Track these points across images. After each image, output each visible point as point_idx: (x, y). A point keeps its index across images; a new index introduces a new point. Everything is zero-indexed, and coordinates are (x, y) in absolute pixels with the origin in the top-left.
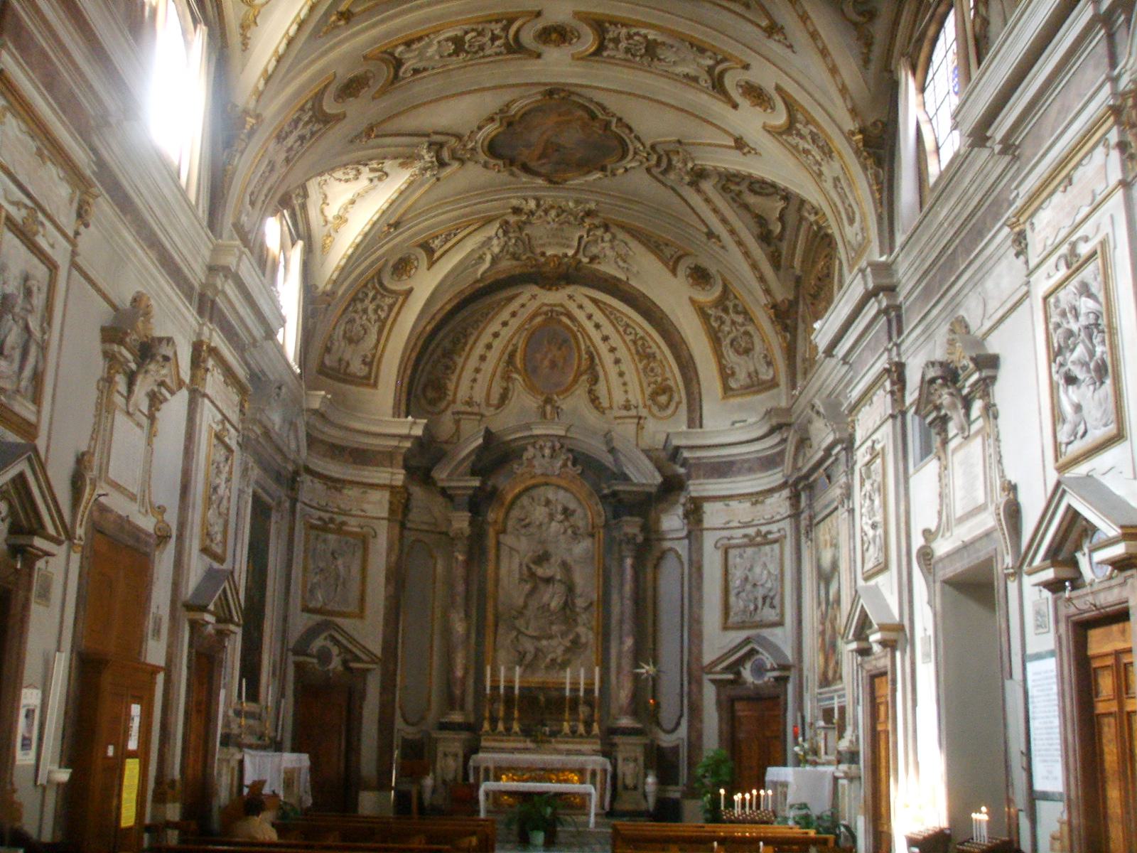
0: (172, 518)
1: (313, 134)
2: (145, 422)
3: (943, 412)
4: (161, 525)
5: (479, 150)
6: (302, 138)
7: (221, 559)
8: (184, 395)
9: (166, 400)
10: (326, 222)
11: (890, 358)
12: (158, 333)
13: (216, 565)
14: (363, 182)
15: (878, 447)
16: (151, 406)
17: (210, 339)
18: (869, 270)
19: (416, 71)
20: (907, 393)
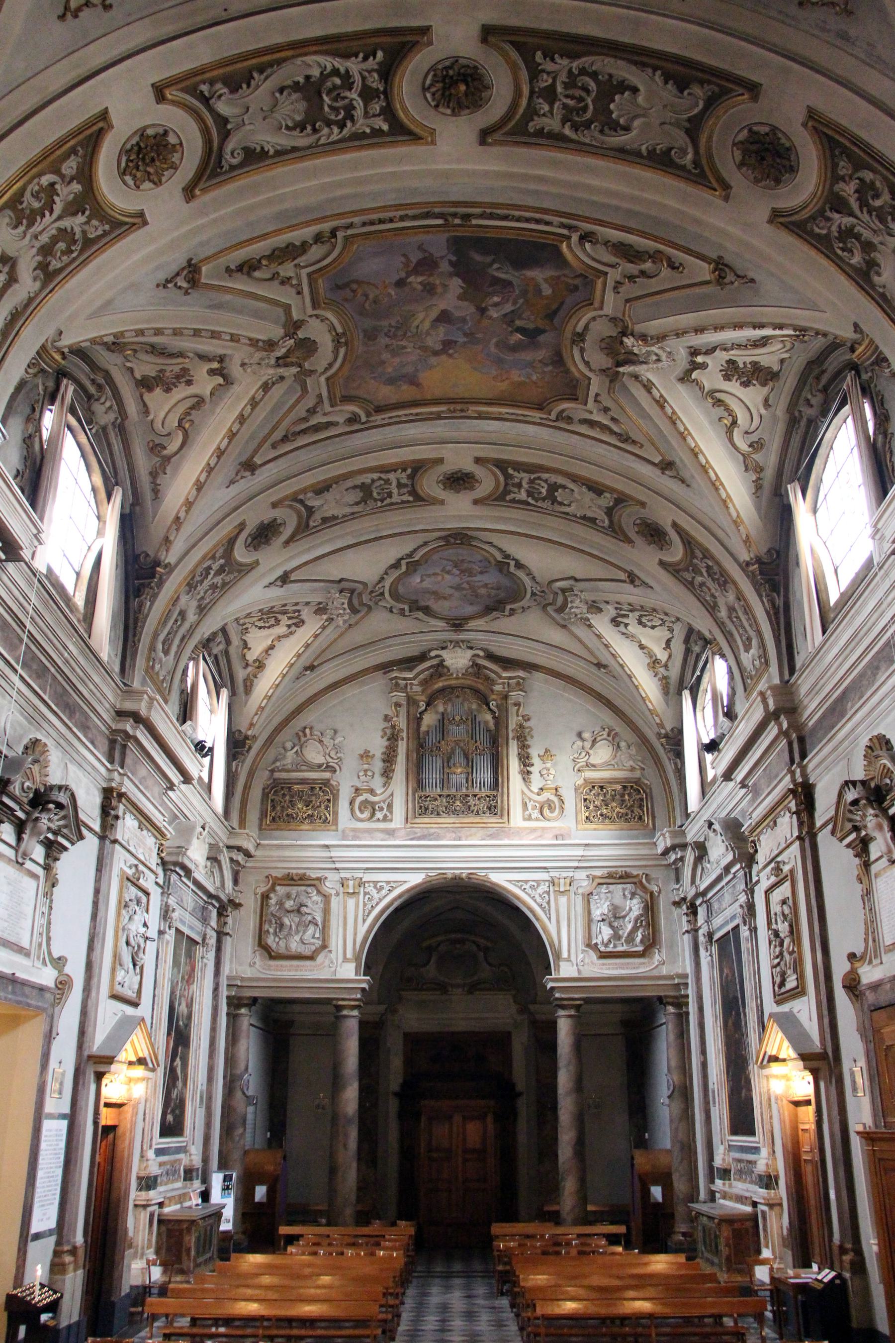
0: (76, 970)
1: (224, 584)
2: (40, 872)
3: (863, 833)
4: (61, 978)
5: (387, 595)
6: (214, 587)
7: (135, 1005)
8: (91, 843)
9: (66, 849)
10: (247, 665)
11: (793, 780)
12: (55, 778)
13: (129, 1010)
14: (281, 630)
15: (786, 869)
16: (47, 856)
17: (121, 784)
18: (769, 692)
19: (325, 520)
20: (817, 815)
